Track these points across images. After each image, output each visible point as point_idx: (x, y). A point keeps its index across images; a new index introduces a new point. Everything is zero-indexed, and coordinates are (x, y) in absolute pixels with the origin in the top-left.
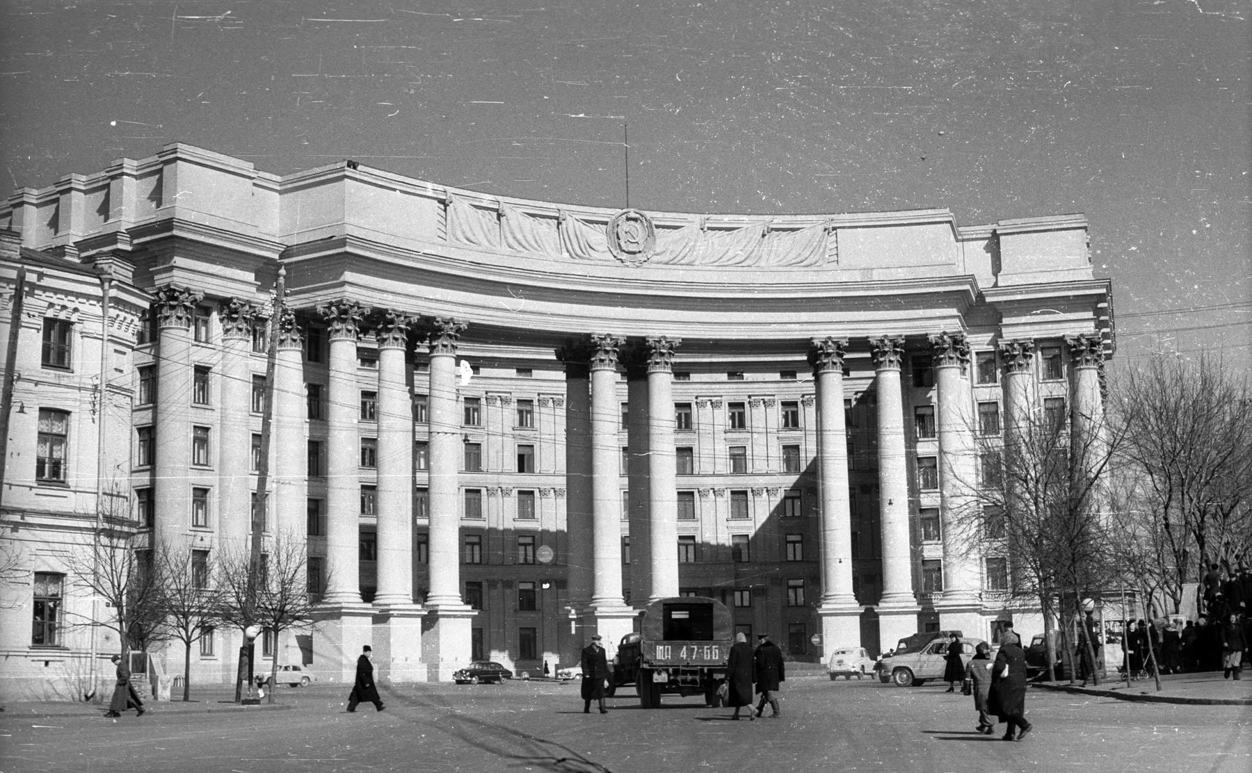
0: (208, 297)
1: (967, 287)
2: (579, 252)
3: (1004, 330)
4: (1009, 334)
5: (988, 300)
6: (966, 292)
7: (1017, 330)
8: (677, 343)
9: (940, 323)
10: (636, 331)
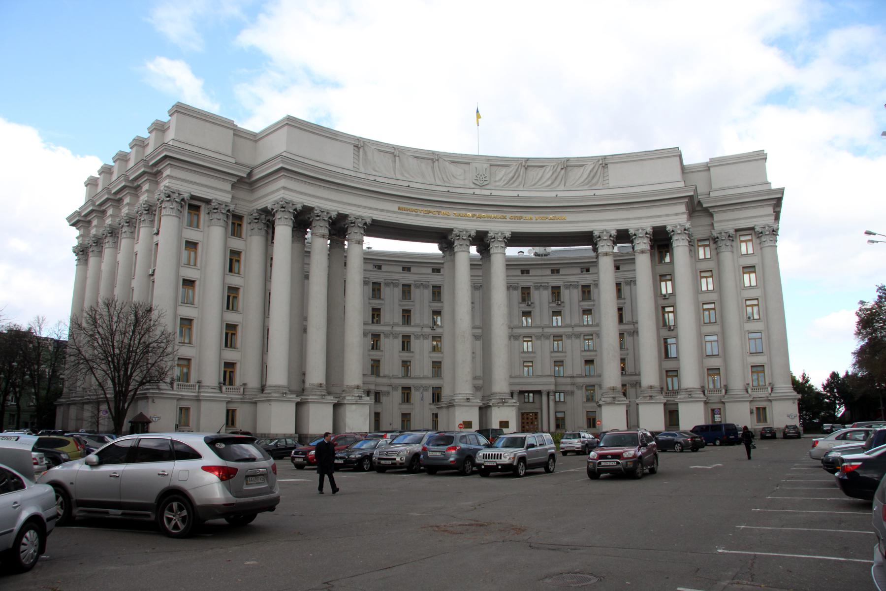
0: (193, 197)
1: (692, 193)
2: (446, 179)
3: (715, 225)
4: (718, 227)
5: (705, 205)
6: (691, 197)
7: (725, 222)
8: (508, 235)
9: (674, 218)
10: (482, 227)
